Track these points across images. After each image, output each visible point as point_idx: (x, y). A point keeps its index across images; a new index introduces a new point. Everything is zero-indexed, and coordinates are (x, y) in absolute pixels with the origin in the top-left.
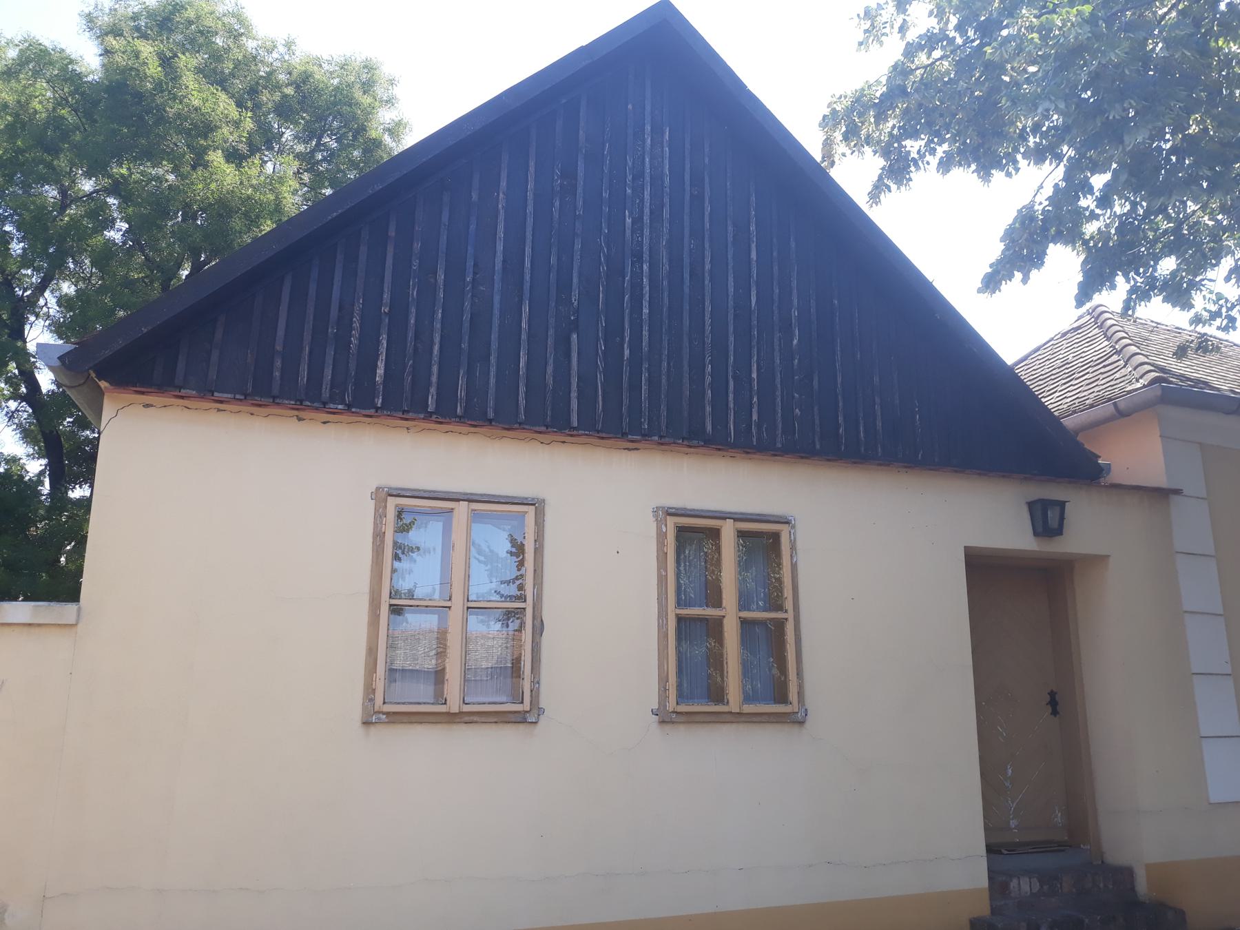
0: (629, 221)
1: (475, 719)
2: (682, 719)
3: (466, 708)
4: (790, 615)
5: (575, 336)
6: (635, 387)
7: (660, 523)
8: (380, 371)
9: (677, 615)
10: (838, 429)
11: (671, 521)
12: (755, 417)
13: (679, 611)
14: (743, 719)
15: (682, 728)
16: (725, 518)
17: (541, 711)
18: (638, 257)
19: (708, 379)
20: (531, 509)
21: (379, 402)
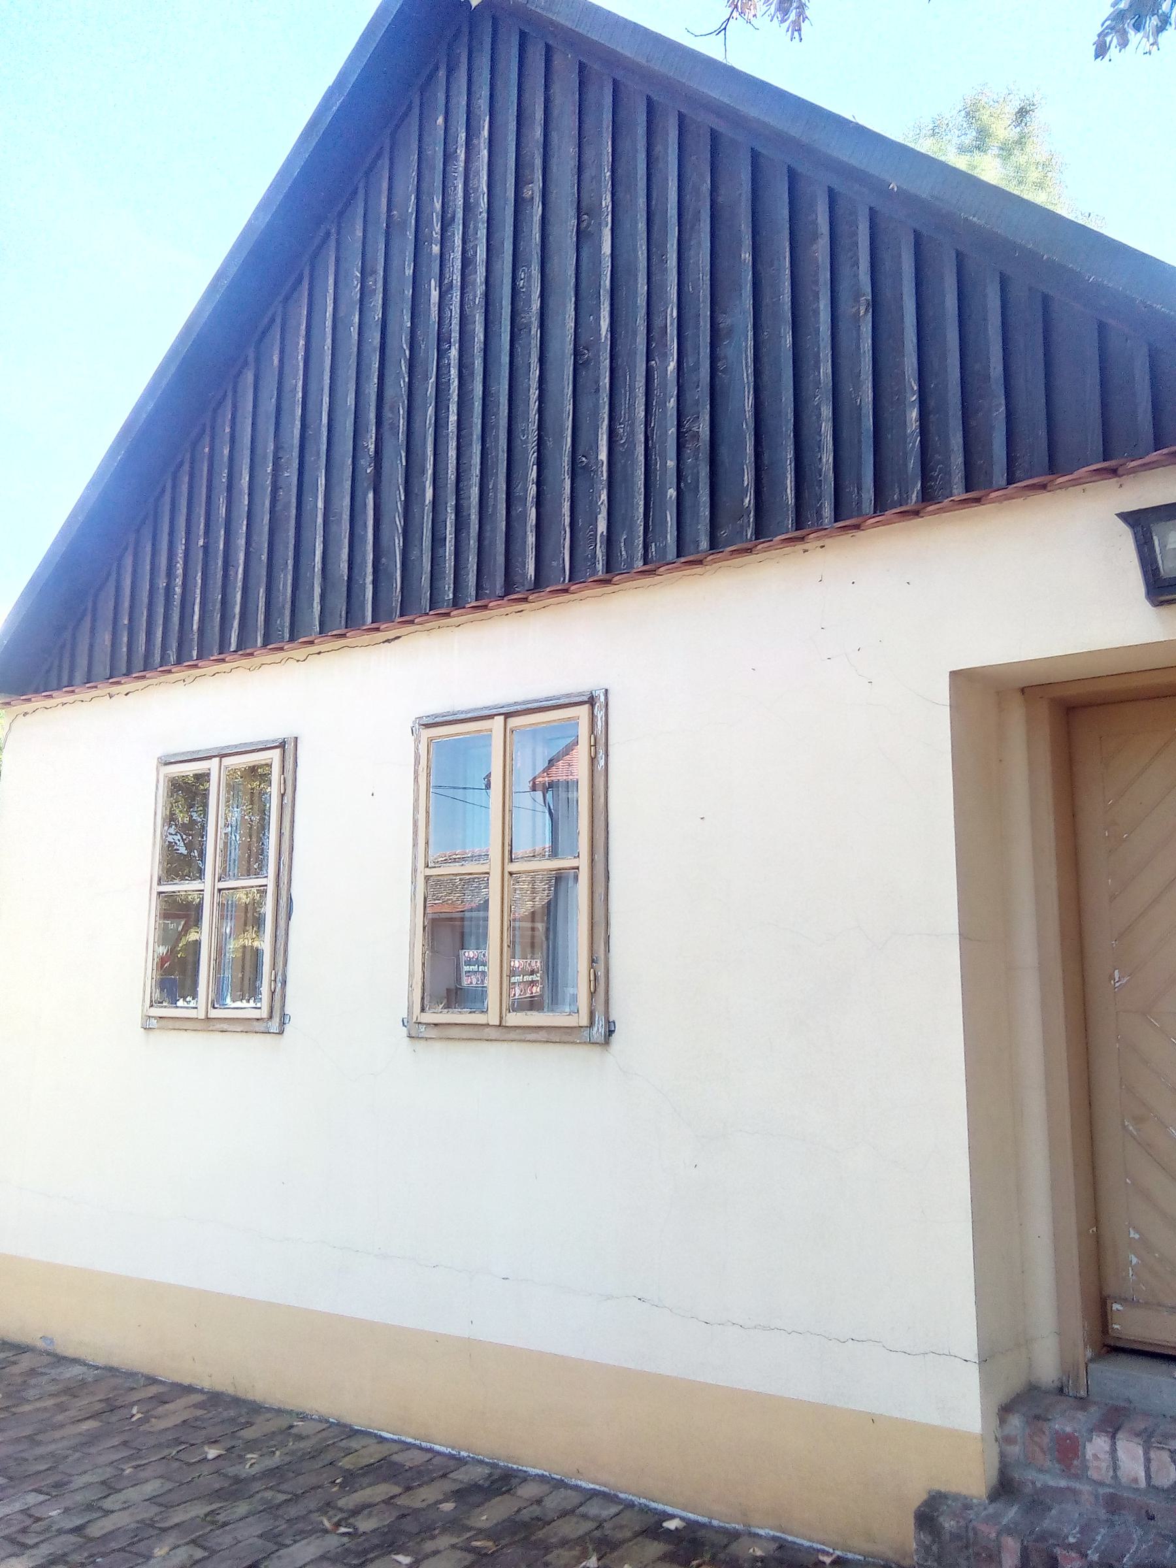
0: (435, 295)
1: (225, 1026)
2: (433, 1033)
3: (214, 1014)
4: (583, 863)
5: (371, 495)
6: (437, 540)
7: (417, 741)
8: (196, 617)
9: (427, 878)
10: (743, 502)
11: (427, 733)
12: (602, 527)
13: (429, 872)
14: (512, 1035)
15: (438, 1045)
16: (491, 717)
17: (284, 1020)
18: (442, 340)
19: (532, 490)
20: (275, 755)
21: (195, 653)
